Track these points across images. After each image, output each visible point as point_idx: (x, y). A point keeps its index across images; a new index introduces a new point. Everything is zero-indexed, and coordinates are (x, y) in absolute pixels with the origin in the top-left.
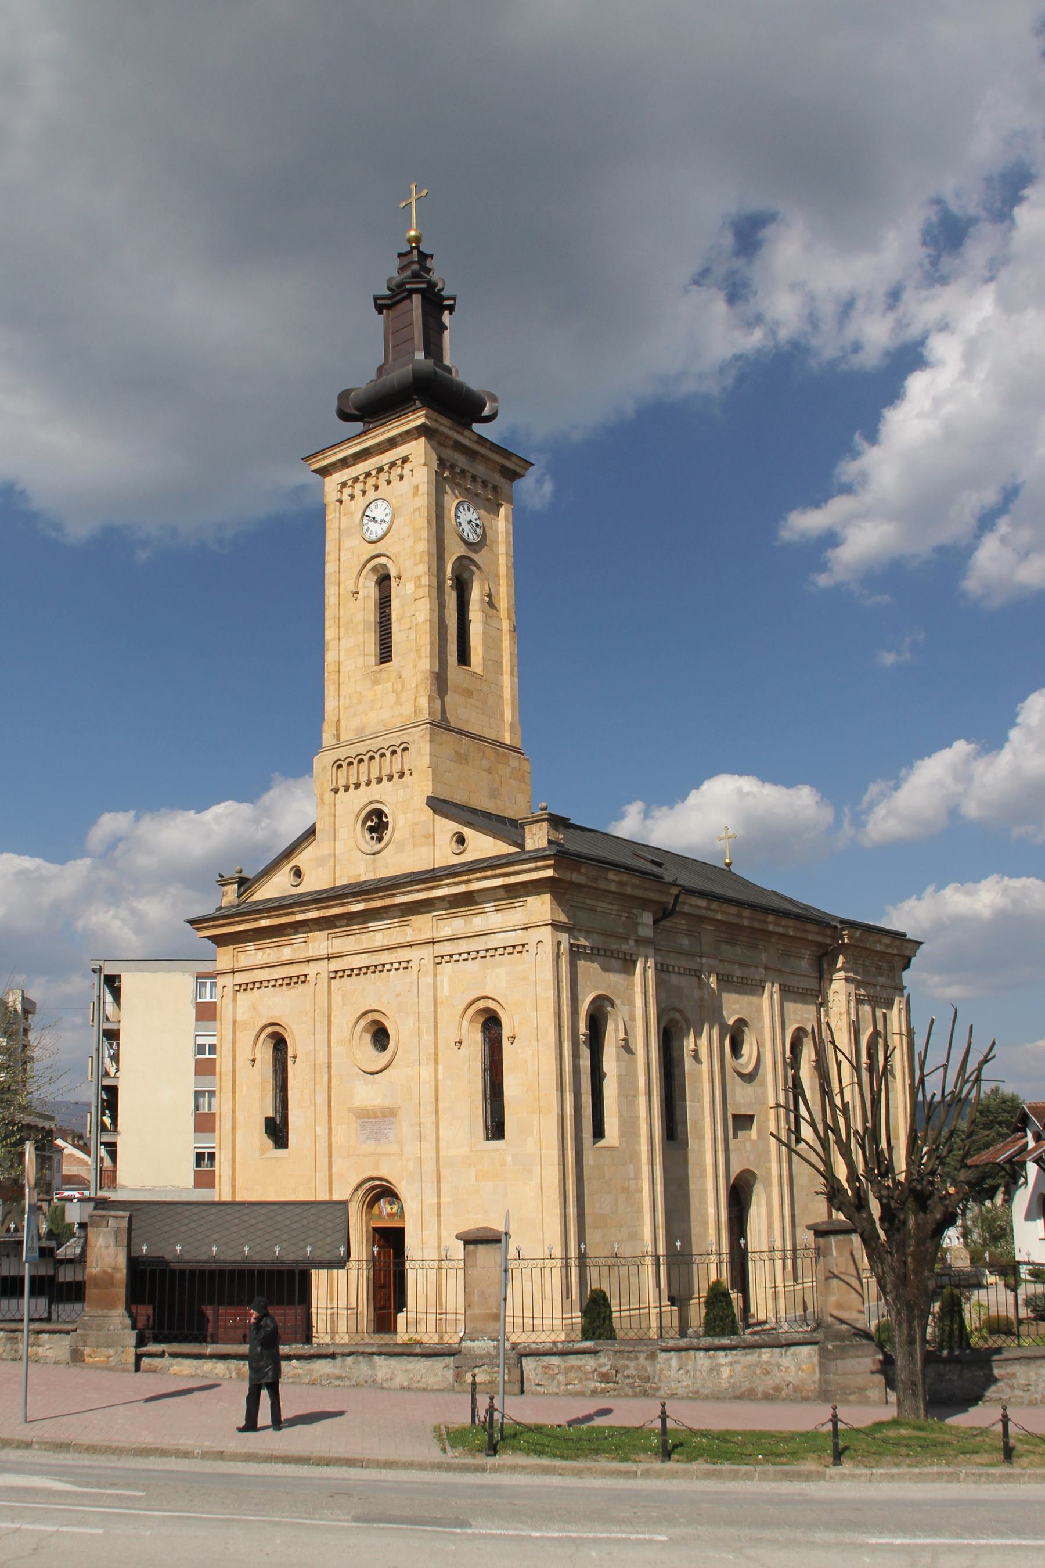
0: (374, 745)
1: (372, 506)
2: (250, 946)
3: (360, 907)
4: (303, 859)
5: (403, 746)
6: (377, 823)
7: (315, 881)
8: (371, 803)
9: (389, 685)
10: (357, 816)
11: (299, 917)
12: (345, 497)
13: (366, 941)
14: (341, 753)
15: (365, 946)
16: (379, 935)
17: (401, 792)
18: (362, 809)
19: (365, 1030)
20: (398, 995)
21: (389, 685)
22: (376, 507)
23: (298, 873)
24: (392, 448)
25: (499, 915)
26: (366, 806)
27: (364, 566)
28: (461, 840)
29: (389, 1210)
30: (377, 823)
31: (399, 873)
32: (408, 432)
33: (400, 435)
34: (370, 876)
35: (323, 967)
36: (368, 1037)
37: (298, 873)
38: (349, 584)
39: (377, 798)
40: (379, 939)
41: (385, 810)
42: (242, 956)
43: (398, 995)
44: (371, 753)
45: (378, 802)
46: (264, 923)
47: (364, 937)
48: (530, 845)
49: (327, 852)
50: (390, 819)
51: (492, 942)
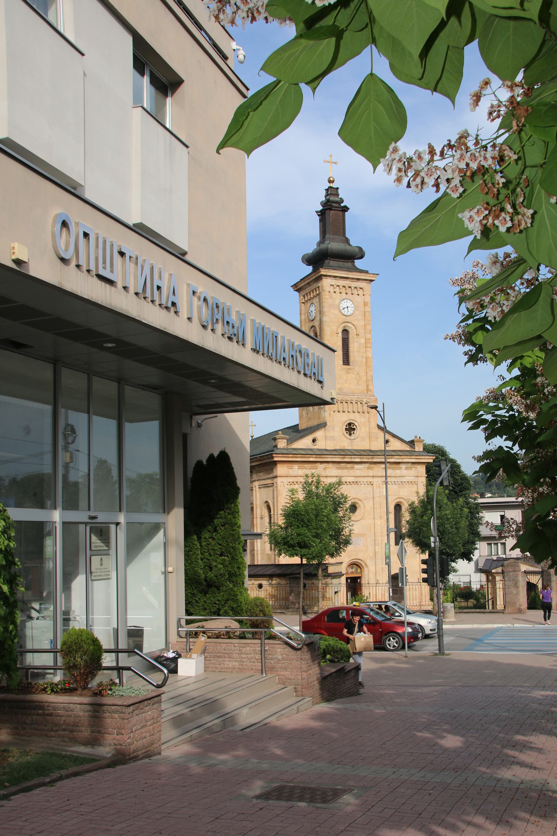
0: (348, 398)
1: (345, 301)
3: (358, 460)
4: (318, 434)
6: (350, 428)
7: (321, 445)
9: (354, 376)
13: (352, 472)
15: (352, 474)
16: (358, 471)
17: (363, 419)
20: (365, 494)
21: (354, 376)
23: (314, 441)
25: (406, 471)
30: (350, 428)
33: (363, 280)
34: (350, 448)
37: (314, 441)
39: (353, 418)
40: (358, 473)
41: (356, 424)
42: (290, 470)
43: (365, 494)
46: (311, 459)
47: (351, 471)
48: (417, 449)
51: (404, 479)
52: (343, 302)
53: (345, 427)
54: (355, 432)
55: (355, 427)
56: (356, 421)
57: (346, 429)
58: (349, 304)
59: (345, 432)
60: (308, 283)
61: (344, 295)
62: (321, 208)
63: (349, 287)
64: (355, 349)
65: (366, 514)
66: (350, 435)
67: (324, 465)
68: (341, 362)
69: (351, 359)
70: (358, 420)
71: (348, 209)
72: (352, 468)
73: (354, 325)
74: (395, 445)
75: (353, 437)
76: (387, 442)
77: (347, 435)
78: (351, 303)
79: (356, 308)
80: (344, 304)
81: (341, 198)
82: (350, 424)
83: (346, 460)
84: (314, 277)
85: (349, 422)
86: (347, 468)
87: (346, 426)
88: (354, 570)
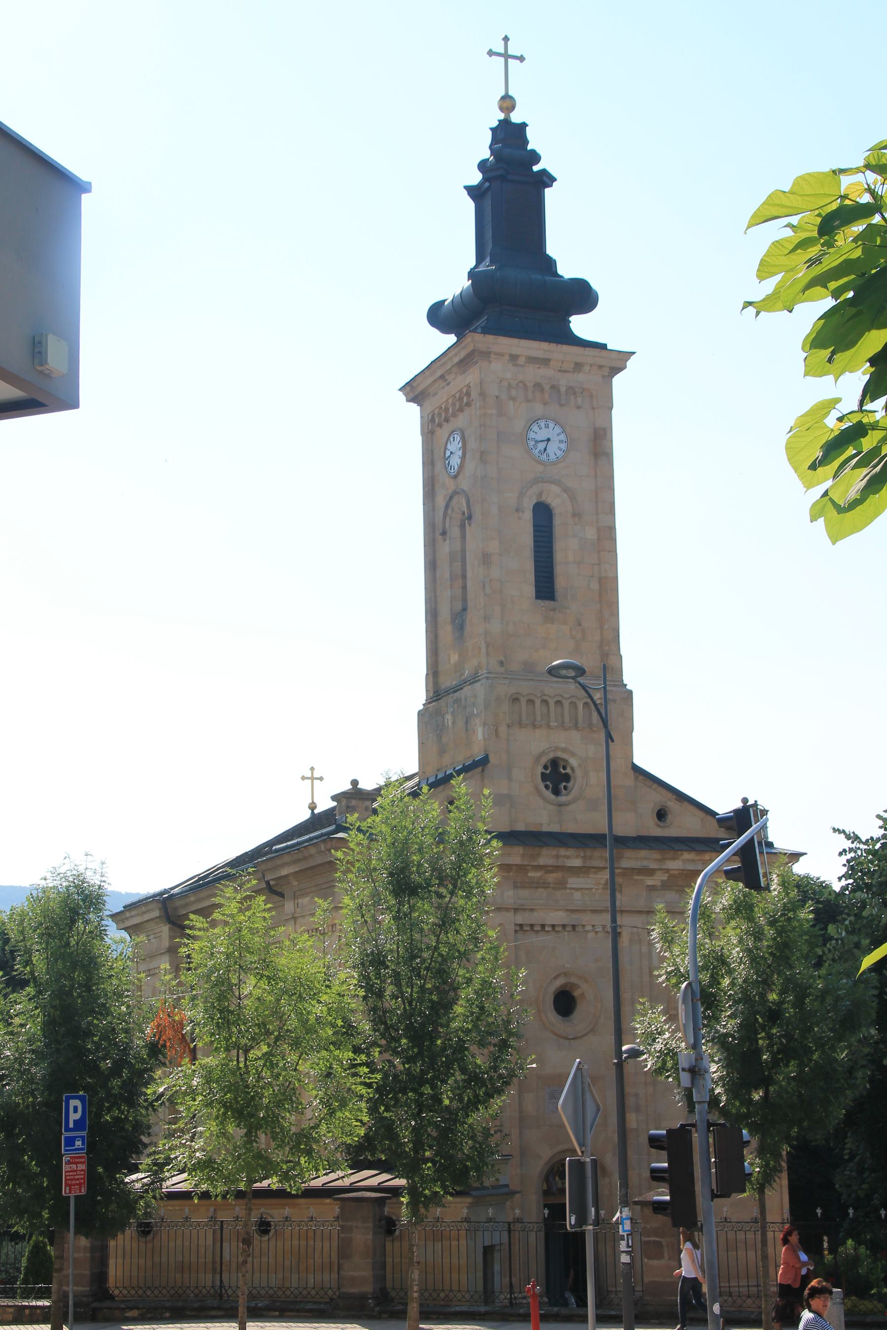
1: (542, 424)
3: (577, 863)
8: (557, 749)
16: (577, 895)
18: (543, 753)
22: (547, 426)
24: (574, 372)
28: (661, 815)
31: (592, 832)
32: (601, 367)
34: (555, 828)
39: (563, 745)
44: (559, 698)
45: (564, 750)
49: (506, 792)
50: (579, 773)
52: (535, 428)
53: (540, 770)
54: (570, 785)
55: (568, 771)
56: (573, 754)
57: (542, 774)
58: (552, 431)
59: (542, 786)
60: (442, 377)
62: (476, 178)
63: (553, 387)
66: (556, 792)
68: (530, 590)
69: (560, 582)
70: (580, 749)
71: (554, 180)
72: (561, 885)
73: (566, 490)
74: (684, 825)
75: (562, 799)
76: (661, 815)
77: (548, 794)
78: (558, 430)
79: (571, 443)
80: (539, 433)
81: (533, 152)
82: (555, 763)
83: (542, 861)
84: (456, 360)
85: (551, 755)
86: (545, 885)
87: (545, 767)
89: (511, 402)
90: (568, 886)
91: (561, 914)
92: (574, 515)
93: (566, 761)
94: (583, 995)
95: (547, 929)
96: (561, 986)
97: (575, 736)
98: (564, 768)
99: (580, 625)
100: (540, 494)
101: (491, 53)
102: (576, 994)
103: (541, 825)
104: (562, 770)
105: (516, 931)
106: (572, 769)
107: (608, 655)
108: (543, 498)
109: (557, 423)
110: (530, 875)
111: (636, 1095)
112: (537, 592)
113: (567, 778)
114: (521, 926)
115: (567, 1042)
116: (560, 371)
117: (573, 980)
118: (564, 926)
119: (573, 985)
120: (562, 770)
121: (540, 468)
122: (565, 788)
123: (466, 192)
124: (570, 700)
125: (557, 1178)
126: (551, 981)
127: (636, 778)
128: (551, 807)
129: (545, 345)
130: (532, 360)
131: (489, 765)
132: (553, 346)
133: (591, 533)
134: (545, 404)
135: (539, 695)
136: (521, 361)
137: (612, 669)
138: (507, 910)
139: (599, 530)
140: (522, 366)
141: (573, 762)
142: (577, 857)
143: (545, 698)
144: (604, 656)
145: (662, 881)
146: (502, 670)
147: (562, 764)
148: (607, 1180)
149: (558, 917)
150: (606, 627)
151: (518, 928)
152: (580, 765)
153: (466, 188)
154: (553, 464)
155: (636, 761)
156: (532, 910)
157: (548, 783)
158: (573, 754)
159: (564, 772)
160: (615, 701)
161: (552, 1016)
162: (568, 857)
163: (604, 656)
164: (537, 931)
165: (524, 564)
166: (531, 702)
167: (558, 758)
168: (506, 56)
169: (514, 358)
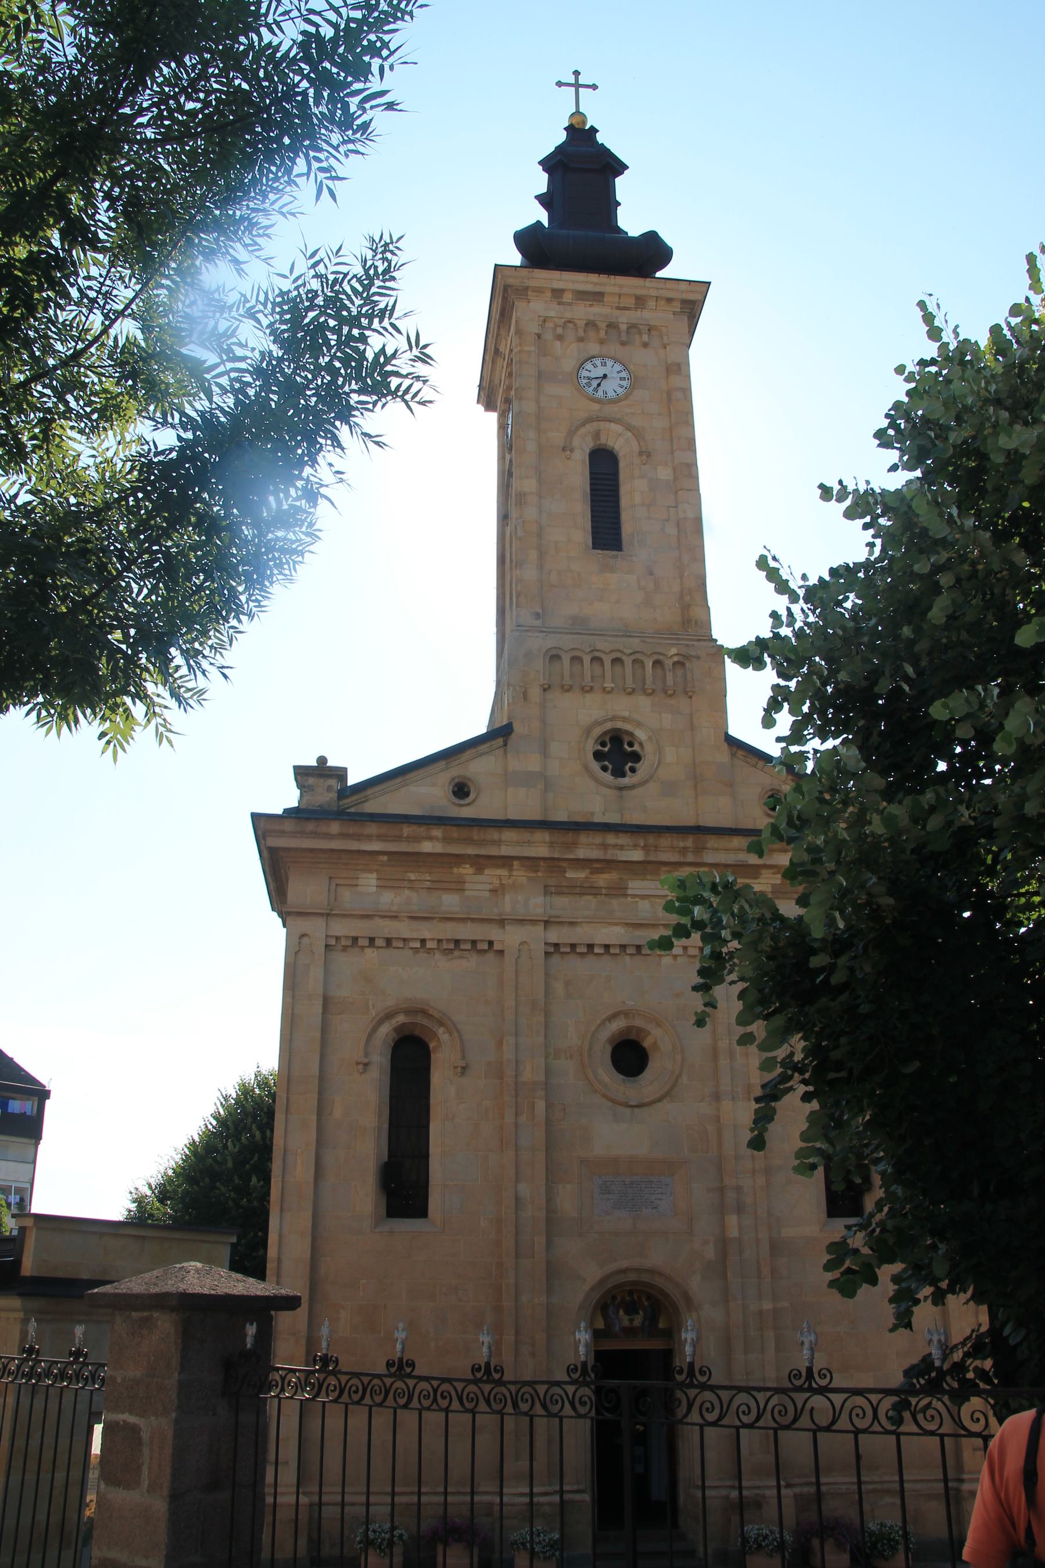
1: (598, 362)
2: (369, 881)
3: (637, 855)
5: (676, 659)
8: (614, 718)
10: (588, 731)
11: (504, 851)
12: (548, 336)
14: (567, 642)
16: (644, 905)
17: (667, 719)
19: (610, 1040)
22: (604, 364)
24: (636, 309)
26: (605, 721)
27: (583, 425)
29: (626, 1323)
32: (669, 300)
35: (537, 937)
36: (609, 1049)
37: (461, 790)
38: (557, 437)
39: (626, 714)
44: (619, 655)
45: (624, 719)
46: (427, 847)
47: (615, 903)
49: (538, 769)
52: (588, 366)
53: (591, 746)
55: (636, 748)
56: (639, 724)
58: (612, 368)
59: (595, 766)
61: (594, 348)
64: (638, 499)
65: (684, 1079)
66: (619, 773)
67: (493, 875)
69: (627, 528)
72: (618, 891)
73: (629, 428)
75: (625, 781)
77: (608, 777)
78: (618, 367)
79: (635, 382)
83: (581, 853)
85: (609, 726)
86: (594, 891)
88: (638, 1320)
89: (558, 343)
90: (630, 892)
91: (618, 930)
92: (641, 453)
93: (631, 734)
94: (655, 1043)
95: (597, 950)
96: (621, 1032)
97: (643, 702)
98: (631, 745)
99: (652, 574)
100: (597, 435)
101: (559, 84)
102: (646, 1044)
103: (592, 814)
104: (626, 746)
105: (547, 954)
106: (641, 744)
107: (689, 606)
108: (603, 441)
109: (616, 360)
110: (568, 875)
111: (738, 1189)
112: (593, 543)
113: (636, 757)
114: (556, 946)
115: (628, 1110)
116: (618, 308)
117: (638, 1023)
118: (623, 947)
119: (640, 1030)
120: (626, 746)
121: (596, 407)
122: (633, 770)
123: (537, 202)
124: (633, 657)
125: (621, 1312)
126: (603, 1023)
127: (733, 755)
128: (608, 791)
129: (593, 278)
130: (582, 295)
131: (513, 735)
132: (604, 278)
133: (664, 474)
134: (602, 342)
135: (588, 650)
136: (568, 297)
137: (696, 622)
138: (533, 922)
139: (674, 469)
140: (570, 304)
141: (640, 734)
142: (635, 846)
143: (597, 654)
144: (686, 608)
145: (773, 885)
146: (538, 623)
147: (626, 739)
148: (694, 1315)
149: (614, 934)
150: (686, 574)
151: (552, 950)
152: (650, 738)
153: (536, 197)
154: (612, 401)
155: (730, 733)
156: (572, 924)
157: (606, 763)
158: (639, 724)
159: (629, 749)
160: (698, 658)
161: (607, 1075)
162: (621, 848)
163: (686, 608)
164: (582, 954)
165: (580, 510)
166: (576, 659)
167: (620, 730)
168: (577, 86)
169: (557, 293)
